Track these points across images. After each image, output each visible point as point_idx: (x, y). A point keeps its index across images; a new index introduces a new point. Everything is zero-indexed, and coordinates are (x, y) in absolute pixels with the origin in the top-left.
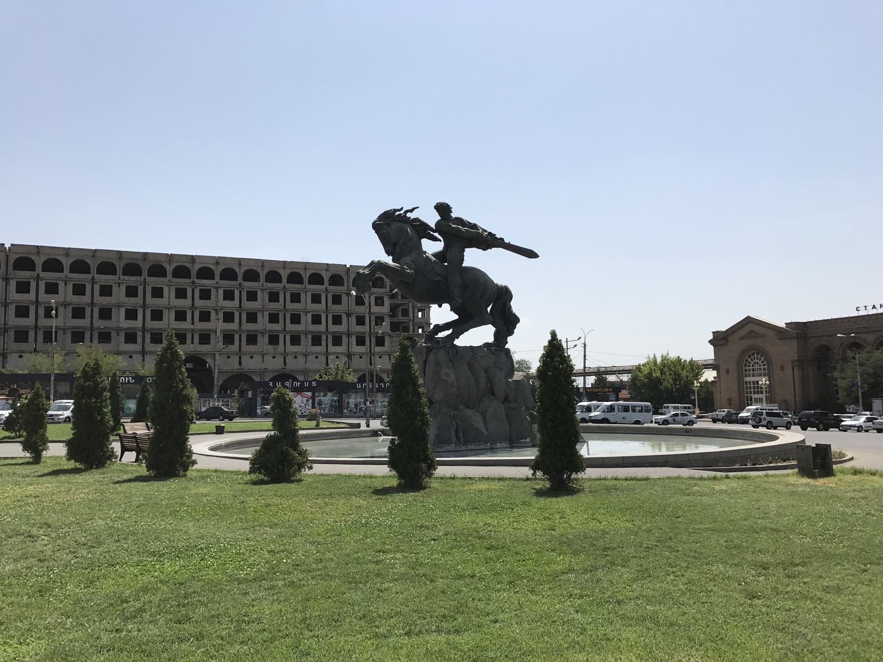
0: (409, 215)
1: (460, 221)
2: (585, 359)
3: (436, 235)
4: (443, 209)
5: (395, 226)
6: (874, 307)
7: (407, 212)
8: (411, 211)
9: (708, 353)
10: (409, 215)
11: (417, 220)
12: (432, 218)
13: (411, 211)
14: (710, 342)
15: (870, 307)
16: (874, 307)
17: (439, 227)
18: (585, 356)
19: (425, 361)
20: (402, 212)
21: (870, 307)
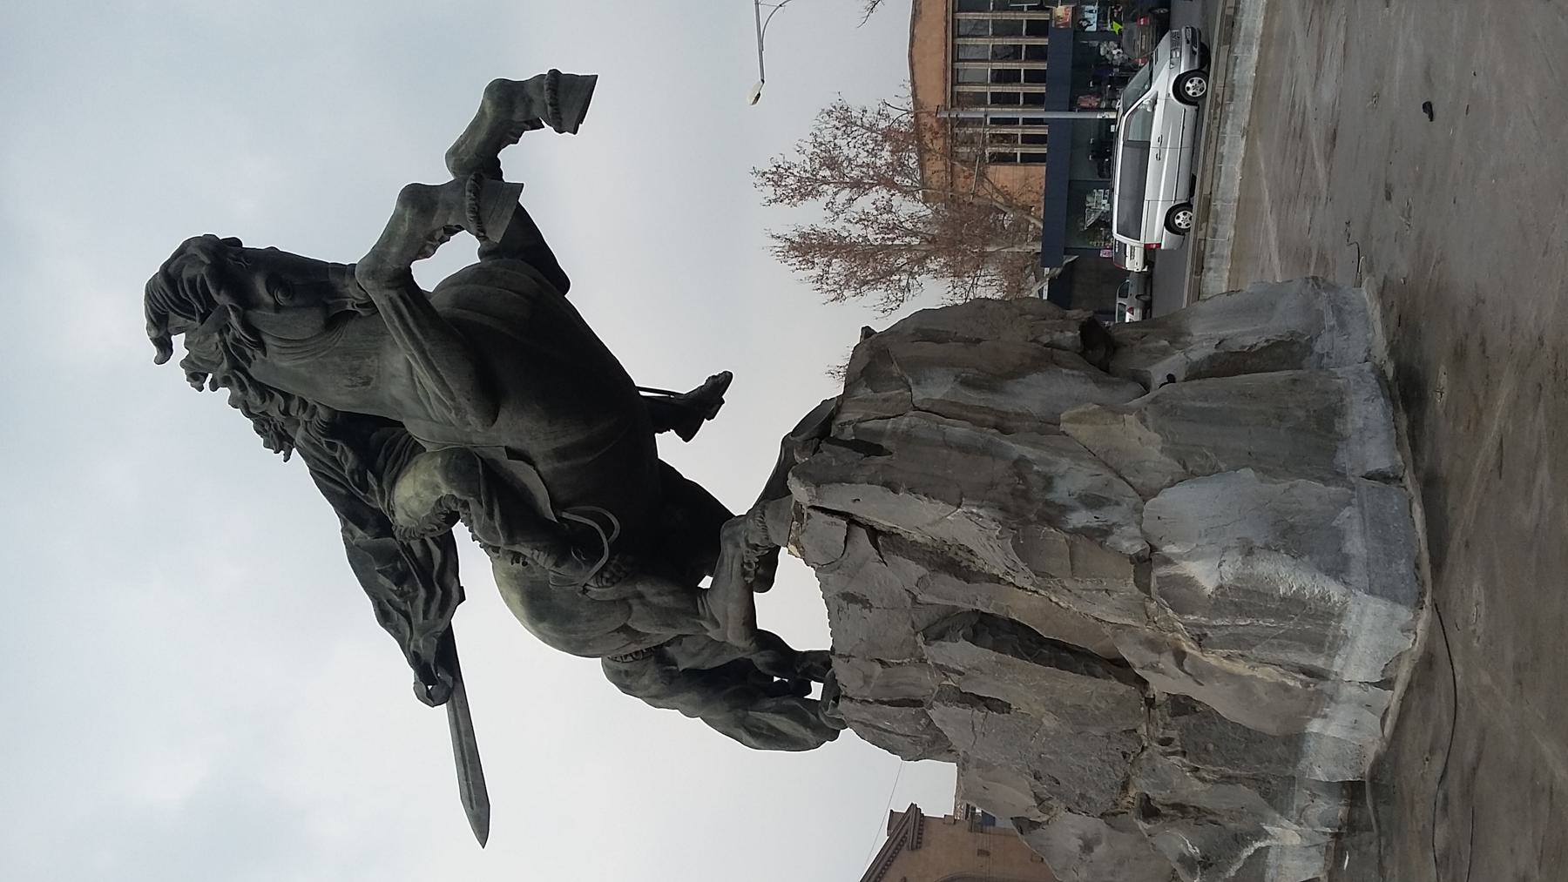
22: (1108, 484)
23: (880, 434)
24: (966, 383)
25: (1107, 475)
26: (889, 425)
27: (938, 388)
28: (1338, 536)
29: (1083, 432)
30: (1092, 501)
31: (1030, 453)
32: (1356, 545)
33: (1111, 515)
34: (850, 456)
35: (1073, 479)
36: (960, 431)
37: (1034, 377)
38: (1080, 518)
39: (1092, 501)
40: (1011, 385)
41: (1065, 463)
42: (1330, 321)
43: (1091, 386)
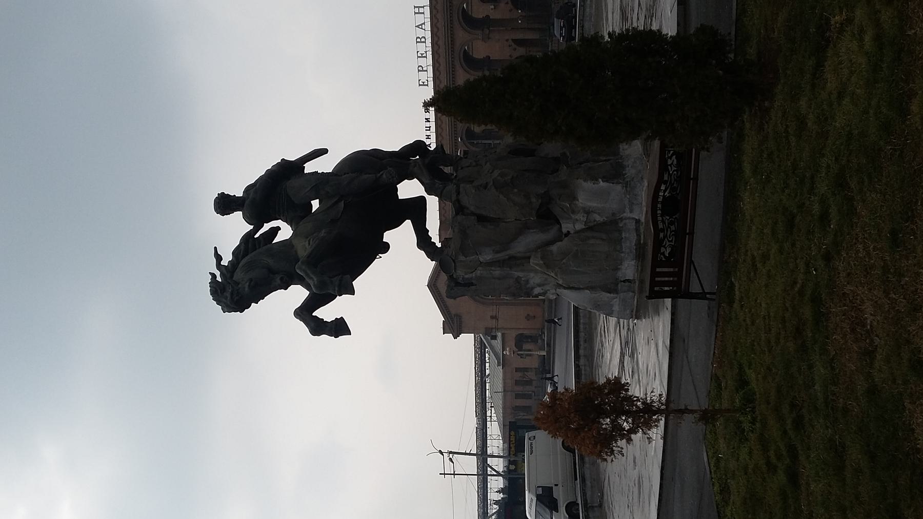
0: (225, 262)
1: (248, 189)
2: (470, 454)
3: (267, 227)
4: (225, 204)
5: (239, 275)
7: (219, 266)
8: (219, 258)
9: (467, 340)
10: (225, 262)
11: (233, 253)
12: (237, 226)
13: (219, 258)
14: (455, 338)
17: (256, 217)
18: (465, 454)
19: (482, 219)
20: (218, 273)
22: (546, 279)
23: (471, 278)
24: (498, 252)
25: (546, 276)
27: (487, 256)
28: (612, 306)
31: (521, 274)
32: (616, 308)
35: (535, 279)
36: (497, 272)
38: (537, 290)
39: (539, 285)
41: (532, 275)
42: (627, 210)
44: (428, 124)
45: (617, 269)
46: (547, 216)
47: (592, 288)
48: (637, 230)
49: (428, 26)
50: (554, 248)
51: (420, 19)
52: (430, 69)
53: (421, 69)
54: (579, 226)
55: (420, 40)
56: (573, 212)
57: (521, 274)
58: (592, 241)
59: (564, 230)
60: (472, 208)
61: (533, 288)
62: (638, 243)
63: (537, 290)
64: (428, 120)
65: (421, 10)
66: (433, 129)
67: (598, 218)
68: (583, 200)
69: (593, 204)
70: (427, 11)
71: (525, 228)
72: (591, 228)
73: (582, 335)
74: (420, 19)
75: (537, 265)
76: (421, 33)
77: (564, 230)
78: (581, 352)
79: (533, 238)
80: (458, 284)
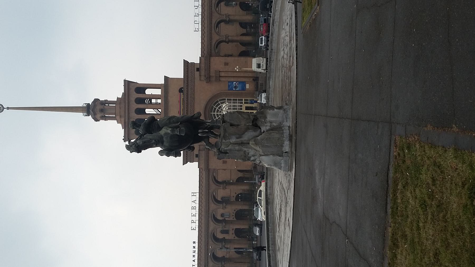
6: (194, 261)
15: (194, 263)
16: (194, 261)
19: (232, 125)
21: (194, 263)
23: (227, 150)
24: (237, 138)
26: (228, 148)
27: (233, 140)
28: (281, 164)
29: (253, 146)
30: (254, 156)
31: (246, 149)
32: (283, 165)
33: (256, 157)
34: (224, 155)
35: (252, 152)
36: (237, 148)
37: (246, 133)
39: (254, 156)
40: (243, 136)
41: (250, 150)
42: (285, 121)
43: (254, 133)
44: (194, 250)
45: (282, 146)
46: (255, 125)
47: (273, 155)
48: (289, 129)
49: (197, 202)
50: (259, 138)
51: (194, 198)
52: (197, 222)
53: (193, 222)
54: (268, 128)
55: (193, 208)
56: (266, 123)
57: (246, 149)
58: (272, 134)
59: (262, 131)
60: (228, 121)
61: (250, 157)
62: (290, 134)
63: (252, 158)
64: (194, 247)
65: (195, 194)
66: (197, 252)
67: (275, 124)
68: (269, 118)
69: (272, 119)
70: (198, 195)
71: (247, 129)
72: (273, 129)
73: (270, 242)
74: (194, 198)
75: (252, 144)
76: (194, 205)
77: (262, 131)
78: (270, 248)
79: (250, 134)
80: (222, 152)
